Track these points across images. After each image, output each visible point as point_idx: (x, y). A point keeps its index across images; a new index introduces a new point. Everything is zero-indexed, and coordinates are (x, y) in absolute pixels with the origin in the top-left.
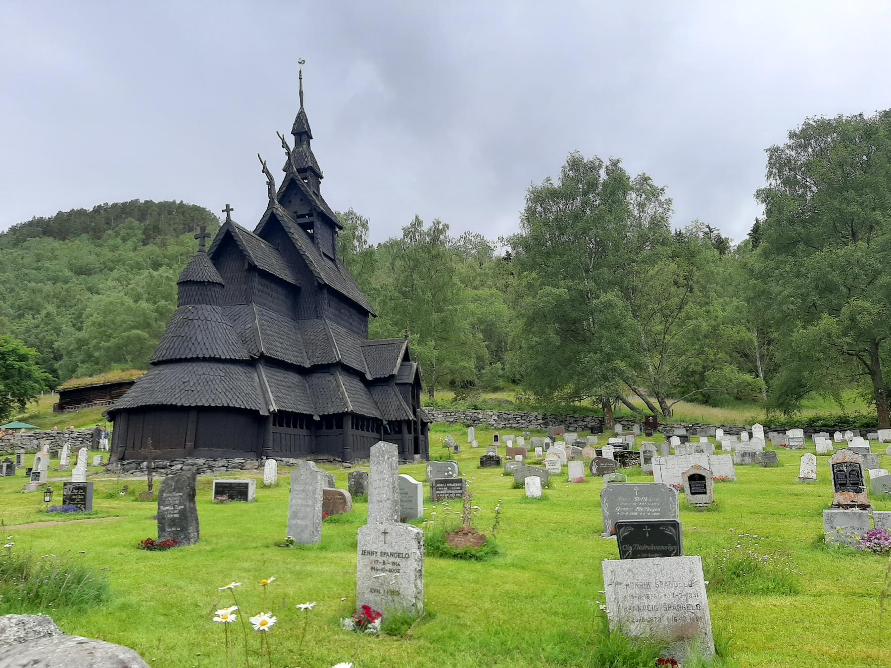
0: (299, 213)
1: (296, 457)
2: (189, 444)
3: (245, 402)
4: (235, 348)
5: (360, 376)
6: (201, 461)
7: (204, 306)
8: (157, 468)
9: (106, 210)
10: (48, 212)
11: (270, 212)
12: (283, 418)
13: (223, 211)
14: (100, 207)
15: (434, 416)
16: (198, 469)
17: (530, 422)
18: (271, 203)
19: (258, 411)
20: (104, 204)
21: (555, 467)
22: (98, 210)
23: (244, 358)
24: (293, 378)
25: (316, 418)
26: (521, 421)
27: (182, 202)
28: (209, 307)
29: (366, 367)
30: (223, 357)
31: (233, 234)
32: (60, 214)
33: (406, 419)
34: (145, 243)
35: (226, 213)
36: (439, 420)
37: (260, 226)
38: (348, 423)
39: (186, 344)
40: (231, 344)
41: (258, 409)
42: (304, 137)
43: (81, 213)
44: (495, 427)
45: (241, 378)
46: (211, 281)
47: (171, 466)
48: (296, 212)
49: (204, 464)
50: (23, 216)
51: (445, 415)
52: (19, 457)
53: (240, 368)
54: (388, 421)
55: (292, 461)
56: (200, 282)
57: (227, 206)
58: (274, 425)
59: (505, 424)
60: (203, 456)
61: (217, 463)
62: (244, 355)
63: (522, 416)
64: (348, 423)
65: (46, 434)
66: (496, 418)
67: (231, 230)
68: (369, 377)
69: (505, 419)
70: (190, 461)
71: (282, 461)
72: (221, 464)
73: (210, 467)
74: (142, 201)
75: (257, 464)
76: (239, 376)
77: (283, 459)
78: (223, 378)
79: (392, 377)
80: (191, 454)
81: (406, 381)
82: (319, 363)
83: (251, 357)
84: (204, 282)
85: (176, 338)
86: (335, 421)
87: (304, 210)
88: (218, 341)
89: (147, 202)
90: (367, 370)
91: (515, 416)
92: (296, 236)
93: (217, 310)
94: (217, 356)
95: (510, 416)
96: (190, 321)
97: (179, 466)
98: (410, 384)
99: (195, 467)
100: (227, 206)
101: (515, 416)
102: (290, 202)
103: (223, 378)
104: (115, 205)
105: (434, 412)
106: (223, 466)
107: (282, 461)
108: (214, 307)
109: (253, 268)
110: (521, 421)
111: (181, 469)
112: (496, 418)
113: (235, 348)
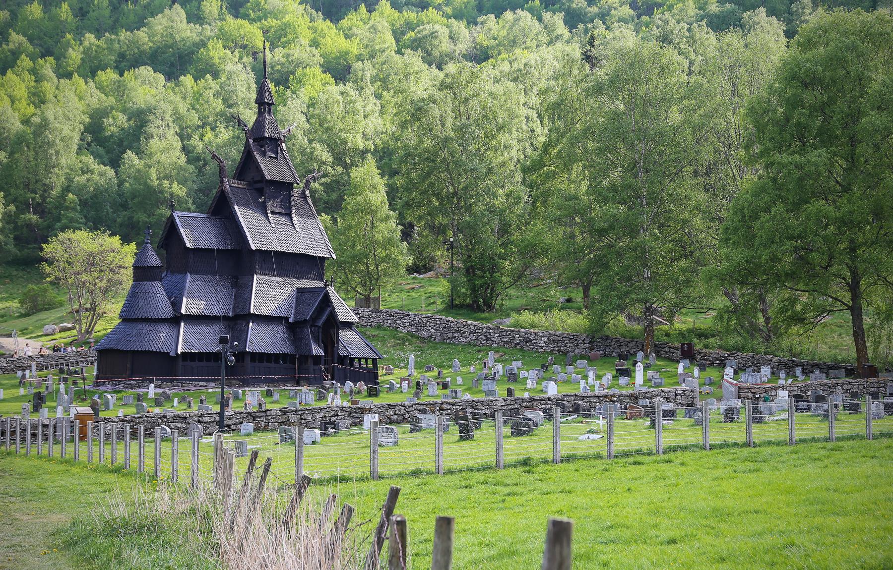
0: (256, 179)
5: (287, 319)
58: (183, 361)
68: (291, 320)
95: (559, 339)
105: (491, 331)
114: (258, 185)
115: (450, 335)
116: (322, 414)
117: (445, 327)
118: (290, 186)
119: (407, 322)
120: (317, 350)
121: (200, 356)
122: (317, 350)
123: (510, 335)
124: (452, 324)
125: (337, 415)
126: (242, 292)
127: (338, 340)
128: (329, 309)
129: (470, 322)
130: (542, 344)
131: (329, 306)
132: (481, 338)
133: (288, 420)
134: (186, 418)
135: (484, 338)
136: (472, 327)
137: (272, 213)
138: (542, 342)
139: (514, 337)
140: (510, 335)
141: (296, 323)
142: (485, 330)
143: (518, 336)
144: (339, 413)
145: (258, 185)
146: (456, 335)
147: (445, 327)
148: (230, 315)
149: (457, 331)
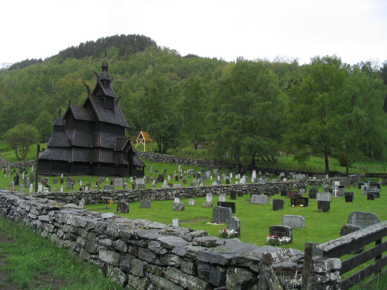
0: (101, 95)
2: (51, 169)
5: (112, 150)
9: (102, 40)
10: (76, 44)
12: (75, 163)
14: (100, 39)
22: (99, 40)
24: (88, 151)
32: (82, 44)
34: (119, 59)
38: (99, 165)
50: (64, 46)
64: (99, 165)
68: (115, 150)
69: (200, 162)
74: (120, 35)
86: (96, 164)
89: (122, 35)
94: (60, 146)
95: (202, 162)
98: (126, 153)
104: (107, 38)
114: (101, 98)
115: (159, 160)
116: (175, 192)
118: (113, 98)
119: (142, 155)
120: (125, 162)
121: (80, 163)
122: (125, 162)
125: (182, 192)
126: (94, 139)
127: (133, 160)
128: (130, 147)
129: (166, 155)
131: (130, 145)
133: (160, 195)
134: (110, 194)
137: (106, 108)
140: (182, 160)
141: (117, 152)
143: (185, 160)
144: (183, 191)
145: (101, 98)
146: (161, 160)
147: (157, 157)
149: (161, 158)
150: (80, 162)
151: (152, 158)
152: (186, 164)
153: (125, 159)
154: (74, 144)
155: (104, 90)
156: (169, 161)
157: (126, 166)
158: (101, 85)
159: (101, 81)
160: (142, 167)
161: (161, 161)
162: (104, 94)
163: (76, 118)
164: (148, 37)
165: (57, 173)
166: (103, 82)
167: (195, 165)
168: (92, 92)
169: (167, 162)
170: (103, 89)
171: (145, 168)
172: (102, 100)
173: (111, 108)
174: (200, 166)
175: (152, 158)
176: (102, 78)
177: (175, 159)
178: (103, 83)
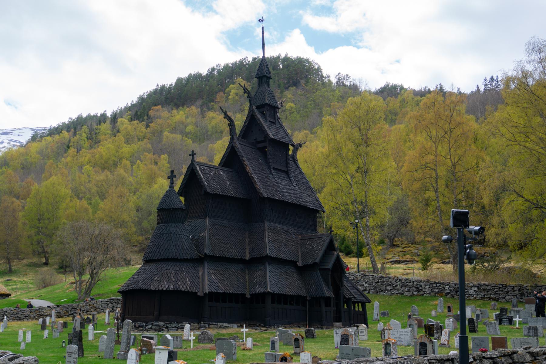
0: (258, 140)
1: (230, 323)
2: (156, 313)
3: (188, 288)
4: (188, 251)
5: (293, 263)
6: (162, 324)
7: (170, 224)
8: (140, 327)
9: (219, 71)
10: (169, 80)
11: (231, 145)
12: (213, 296)
13: (190, 155)
15: (421, 287)
16: (160, 329)
17: (507, 293)
18: (232, 139)
19: (197, 293)
20: (217, 66)
21: (363, 334)
23: (194, 258)
25: (248, 296)
26: (499, 292)
27: (286, 56)
28: (173, 225)
29: (300, 256)
30: (179, 258)
31: (195, 171)
32: (179, 80)
33: (323, 296)
35: (191, 156)
36: (426, 290)
37: (225, 155)
38: (269, 300)
39: (158, 250)
40: (185, 248)
41: (197, 291)
42: (265, 79)
43: (198, 77)
44: (475, 298)
45: (190, 271)
46: (175, 208)
47: (146, 326)
48: (255, 140)
49: (164, 325)
51: (431, 286)
52: (93, 317)
53: (191, 265)
54: (311, 297)
55: (225, 325)
56: (168, 209)
57: (193, 151)
59: (484, 295)
60: (165, 321)
61: (171, 325)
62: (195, 254)
63: (500, 287)
64: (269, 300)
65: (117, 300)
66: (476, 289)
67: (194, 168)
68: (300, 264)
69: (484, 290)
70: (155, 324)
71: (217, 325)
72: (173, 326)
73: (167, 328)
75: (198, 326)
76: (189, 270)
77: (219, 323)
78: (178, 272)
79: (315, 264)
80: (158, 320)
81: (327, 267)
82: (255, 256)
83: (199, 256)
84: (170, 208)
85: (153, 246)
86: (260, 298)
87: (262, 139)
88: (177, 247)
90: (300, 259)
91: (493, 288)
92: (247, 163)
93: (179, 227)
94: (176, 258)
95: (488, 288)
96: (162, 235)
97: (150, 326)
98: (329, 269)
99: (158, 328)
100: (193, 151)
101: (493, 288)
102: (252, 131)
103: (178, 272)
104: (226, 67)
105: (422, 284)
106: (175, 327)
107: (217, 325)
108: (177, 224)
109: (207, 194)
110: (499, 292)
111: (151, 328)
112: (476, 289)
113: (188, 251)
115: (383, 288)
117: (378, 282)
120: (328, 293)
122: (328, 293)
123: (440, 286)
124: (384, 279)
127: (342, 285)
130: (472, 292)
132: (413, 290)
135: (415, 289)
136: (403, 281)
137: (274, 169)
138: (472, 291)
139: (444, 288)
140: (440, 286)
142: (415, 283)
143: (448, 287)
146: (389, 288)
148: (247, 258)
149: (390, 285)
150: (224, 293)
151: (366, 285)
152: (449, 296)
153: (327, 285)
154: (207, 251)
155: (266, 127)
156: (409, 291)
157: (327, 300)
158: (259, 116)
159: (258, 107)
160: (360, 304)
161: (387, 290)
162: (267, 135)
163: (208, 190)
164: (305, 58)
165: (170, 323)
166: (261, 110)
167: (473, 296)
168: (238, 130)
169: (402, 294)
170: (262, 124)
171: (366, 304)
172: (262, 151)
173: (285, 170)
174: (482, 298)
175: (366, 285)
176: (259, 103)
177: (421, 286)
178: (262, 113)
